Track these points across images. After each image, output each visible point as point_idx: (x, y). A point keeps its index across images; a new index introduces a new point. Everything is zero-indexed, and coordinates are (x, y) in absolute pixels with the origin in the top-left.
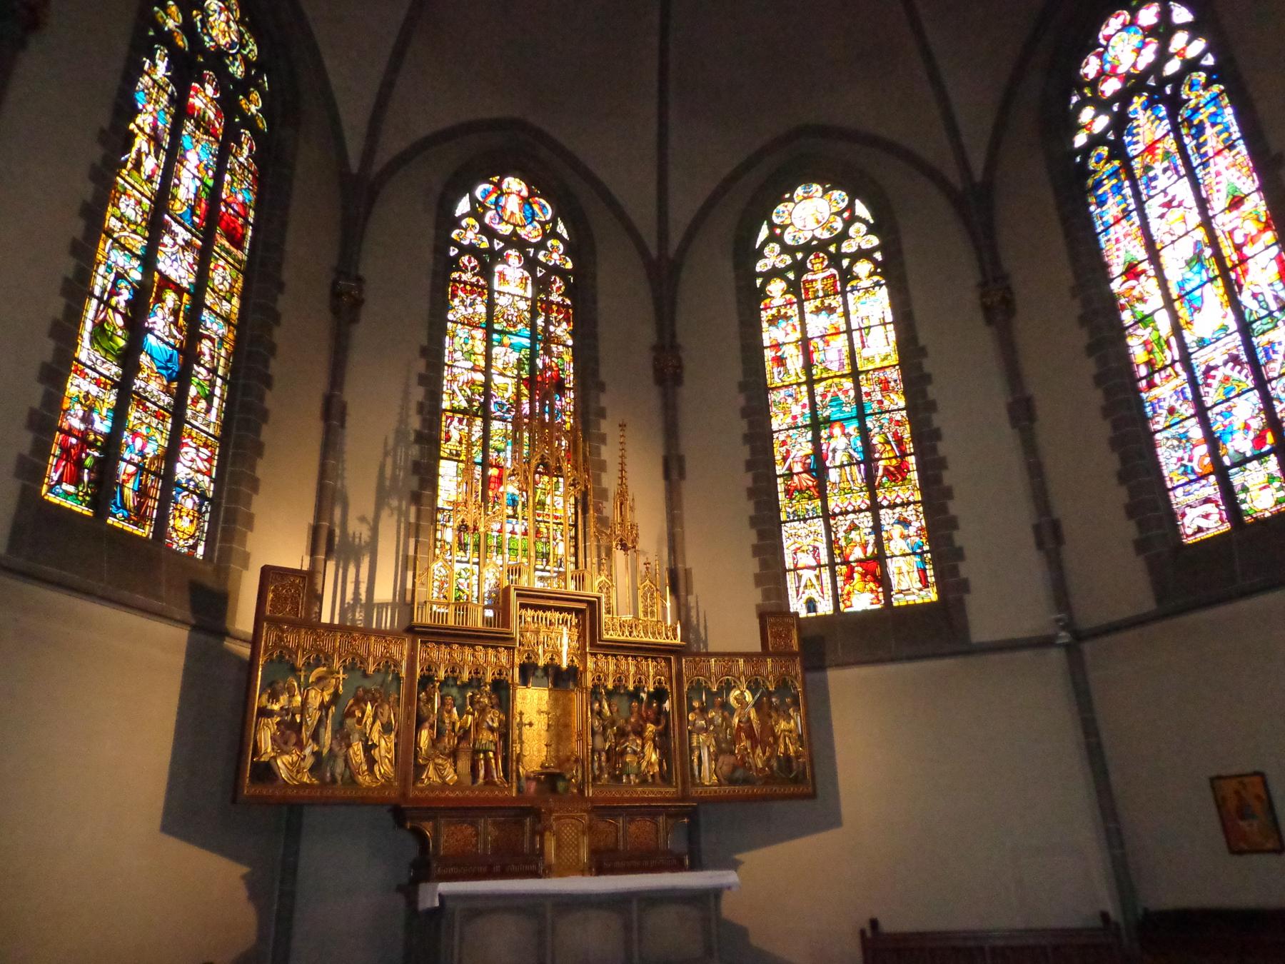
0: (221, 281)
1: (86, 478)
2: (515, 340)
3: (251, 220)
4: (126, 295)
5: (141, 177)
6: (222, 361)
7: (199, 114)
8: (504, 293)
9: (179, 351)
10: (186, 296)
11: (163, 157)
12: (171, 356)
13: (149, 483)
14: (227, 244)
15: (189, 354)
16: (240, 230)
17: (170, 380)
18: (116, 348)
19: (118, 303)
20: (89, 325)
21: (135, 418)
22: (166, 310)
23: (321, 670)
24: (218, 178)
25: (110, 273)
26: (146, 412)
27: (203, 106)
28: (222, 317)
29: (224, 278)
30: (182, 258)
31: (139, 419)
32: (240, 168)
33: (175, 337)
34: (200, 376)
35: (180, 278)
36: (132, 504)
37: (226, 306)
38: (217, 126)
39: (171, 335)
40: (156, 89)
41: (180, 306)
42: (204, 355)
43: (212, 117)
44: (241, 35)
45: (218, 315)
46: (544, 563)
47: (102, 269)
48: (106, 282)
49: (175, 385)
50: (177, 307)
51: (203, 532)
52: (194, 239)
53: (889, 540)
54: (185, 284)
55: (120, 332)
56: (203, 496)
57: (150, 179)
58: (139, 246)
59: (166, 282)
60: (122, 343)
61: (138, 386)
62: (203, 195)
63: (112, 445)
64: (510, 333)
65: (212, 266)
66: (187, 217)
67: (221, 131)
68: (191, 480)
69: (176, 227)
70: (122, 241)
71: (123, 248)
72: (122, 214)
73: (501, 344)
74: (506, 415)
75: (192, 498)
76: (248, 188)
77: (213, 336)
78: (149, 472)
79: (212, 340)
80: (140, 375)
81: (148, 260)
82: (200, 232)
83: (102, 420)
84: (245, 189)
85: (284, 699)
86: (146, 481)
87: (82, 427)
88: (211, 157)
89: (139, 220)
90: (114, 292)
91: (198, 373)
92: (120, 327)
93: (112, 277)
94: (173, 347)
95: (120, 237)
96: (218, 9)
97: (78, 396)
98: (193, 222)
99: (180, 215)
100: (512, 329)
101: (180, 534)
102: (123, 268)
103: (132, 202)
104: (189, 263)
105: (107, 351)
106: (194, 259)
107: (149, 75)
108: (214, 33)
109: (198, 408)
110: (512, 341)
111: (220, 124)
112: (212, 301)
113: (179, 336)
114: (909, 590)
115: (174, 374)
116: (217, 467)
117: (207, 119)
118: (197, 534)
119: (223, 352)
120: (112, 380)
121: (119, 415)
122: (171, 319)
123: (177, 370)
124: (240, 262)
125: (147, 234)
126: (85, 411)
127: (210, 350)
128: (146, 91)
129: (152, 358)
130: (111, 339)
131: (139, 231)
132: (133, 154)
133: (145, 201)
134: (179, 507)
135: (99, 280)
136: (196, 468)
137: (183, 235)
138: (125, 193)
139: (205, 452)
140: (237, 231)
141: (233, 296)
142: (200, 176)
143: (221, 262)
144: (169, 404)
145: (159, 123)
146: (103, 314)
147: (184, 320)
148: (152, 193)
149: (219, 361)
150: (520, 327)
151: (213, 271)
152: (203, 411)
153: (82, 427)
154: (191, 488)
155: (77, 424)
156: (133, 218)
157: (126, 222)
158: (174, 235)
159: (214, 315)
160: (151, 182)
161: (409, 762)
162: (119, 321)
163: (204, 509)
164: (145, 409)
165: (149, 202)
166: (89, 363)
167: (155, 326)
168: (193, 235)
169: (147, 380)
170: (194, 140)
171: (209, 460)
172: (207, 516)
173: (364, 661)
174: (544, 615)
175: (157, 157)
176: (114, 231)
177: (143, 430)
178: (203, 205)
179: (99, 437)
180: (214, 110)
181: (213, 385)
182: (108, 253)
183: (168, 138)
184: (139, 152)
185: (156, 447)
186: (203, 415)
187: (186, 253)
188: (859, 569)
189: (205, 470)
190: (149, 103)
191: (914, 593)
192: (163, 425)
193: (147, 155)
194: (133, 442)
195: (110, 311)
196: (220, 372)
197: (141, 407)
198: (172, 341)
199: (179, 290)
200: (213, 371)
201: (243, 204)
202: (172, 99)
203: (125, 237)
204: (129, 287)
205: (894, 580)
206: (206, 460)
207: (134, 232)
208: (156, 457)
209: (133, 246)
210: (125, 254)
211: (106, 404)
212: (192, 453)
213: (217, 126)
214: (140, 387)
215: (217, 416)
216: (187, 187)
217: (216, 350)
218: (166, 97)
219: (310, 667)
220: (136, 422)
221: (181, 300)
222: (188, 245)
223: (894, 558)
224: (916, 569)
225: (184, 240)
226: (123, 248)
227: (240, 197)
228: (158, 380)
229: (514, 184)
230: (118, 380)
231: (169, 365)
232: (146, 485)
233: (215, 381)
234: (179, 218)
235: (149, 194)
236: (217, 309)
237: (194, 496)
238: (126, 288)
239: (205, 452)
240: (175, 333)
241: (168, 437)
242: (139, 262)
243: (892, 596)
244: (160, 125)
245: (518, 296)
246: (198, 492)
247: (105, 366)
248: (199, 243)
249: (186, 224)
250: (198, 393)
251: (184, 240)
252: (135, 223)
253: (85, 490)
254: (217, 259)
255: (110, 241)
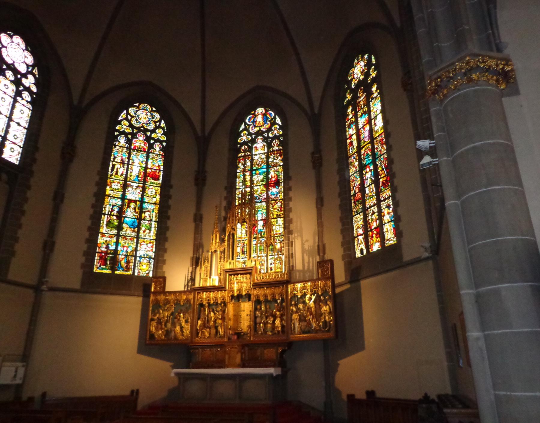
0: (151, 192)
1: (108, 263)
2: (261, 171)
3: (162, 169)
4: (116, 210)
5: (118, 176)
6: (154, 216)
7: (137, 147)
8: (256, 155)
9: (137, 219)
10: (138, 203)
11: (126, 166)
12: (134, 221)
13: (130, 259)
14: (153, 181)
15: (140, 219)
16: (158, 174)
17: (134, 228)
18: (114, 225)
19: (114, 213)
20: (105, 223)
21: (123, 242)
22: (131, 209)
23: (168, 306)
24: (147, 163)
25: (110, 206)
26: (127, 240)
27: (139, 144)
28: (153, 203)
29: (152, 192)
30: (136, 192)
31: (125, 242)
32: (156, 155)
33: (135, 215)
34: (145, 224)
35: (135, 198)
36: (124, 266)
37: (154, 199)
38: (145, 147)
39: (134, 215)
40: (121, 148)
41: (136, 206)
42: (146, 217)
43: (143, 145)
44: (152, 115)
45: (151, 203)
46: (272, 252)
47: (108, 206)
48: (109, 209)
49: (137, 229)
50: (135, 207)
51: (151, 268)
52: (140, 184)
53: (384, 216)
54: (137, 199)
55: (115, 221)
56: (150, 258)
57: (122, 175)
58: (120, 195)
59: (130, 201)
60: (116, 224)
61: (123, 233)
62: (142, 170)
63: (116, 251)
64: (259, 169)
65: (147, 190)
66: (137, 179)
67: (147, 148)
68: (146, 254)
69: (132, 184)
70: (114, 196)
71: (114, 197)
72: (113, 189)
73: (256, 174)
74: (258, 200)
75: (146, 259)
76: (160, 160)
77: (150, 210)
78: (129, 256)
79: (149, 211)
80: (123, 230)
81: (123, 198)
82: (142, 181)
83: (112, 246)
84: (159, 161)
85: (157, 315)
86: (129, 258)
87: (106, 250)
88: (144, 158)
89: (119, 187)
90: (112, 210)
91: (145, 223)
92: (115, 220)
93: (111, 207)
94: (134, 218)
95: (113, 195)
96: (142, 112)
97: (103, 242)
98: (139, 180)
99: (134, 180)
100: (259, 167)
101: (143, 271)
102: (115, 203)
103: (116, 183)
104: (138, 192)
105: (111, 227)
106: (140, 190)
107: (118, 146)
108: (141, 121)
109: (146, 233)
110: (260, 172)
111: (146, 146)
112: (148, 200)
113: (136, 215)
114: (390, 239)
115: (136, 226)
116: (155, 248)
117: (141, 147)
118: (149, 269)
119: (154, 214)
120: (114, 235)
121: (117, 243)
122: (134, 211)
123: (136, 225)
124: (159, 184)
125: (122, 190)
126: (106, 246)
127: (149, 215)
128: (118, 151)
129: (127, 224)
130: (113, 224)
131: (119, 191)
132: (115, 170)
133: (120, 181)
134: (141, 263)
135: (107, 209)
136: (147, 250)
137: (135, 185)
138: (114, 182)
139: (150, 245)
140: (157, 175)
141: (156, 195)
142: (140, 165)
143: (151, 187)
144: (135, 235)
145: (123, 157)
146: (110, 218)
147: (138, 209)
148: (123, 178)
149: (152, 216)
150: (262, 165)
151: (148, 191)
152: (148, 233)
153: (106, 250)
154: (145, 256)
155: (104, 249)
156: (117, 188)
157: (115, 190)
158: (132, 187)
159: (149, 204)
160: (122, 175)
161: (195, 332)
162: (115, 218)
163: (151, 261)
164: (126, 239)
165: (122, 181)
166: (106, 232)
167: (128, 215)
168: (139, 183)
169: (126, 231)
170: (137, 156)
171: (152, 247)
172: (152, 263)
173: (180, 301)
174: (243, 276)
175: (124, 167)
176: (111, 194)
177: (126, 245)
178: (142, 173)
179: (111, 251)
180: (143, 143)
181: (151, 224)
182: (109, 201)
183: (127, 160)
184: (117, 169)
185: (132, 248)
186: (148, 234)
187: (137, 190)
188: (375, 232)
189: (150, 250)
190: (119, 154)
191: (392, 240)
192: (133, 242)
193: (120, 168)
194: (123, 249)
195: (112, 216)
196: (154, 220)
197: (125, 239)
198: (134, 217)
199: (135, 201)
200: (151, 220)
201: (159, 166)
202: (127, 148)
203: (115, 194)
204: (117, 207)
205: (386, 235)
206: (151, 247)
207: (118, 192)
208: (132, 251)
209: (118, 196)
210: (115, 199)
211: (113, 242)
212: (145, 246)
213: (145, 147)
214: (124, 234)
215: (154, 233)
216: (135, 170)
217: (151, 214)
218: (125, 149)
219: (165, 305)
220: (124, 243)
221: (136, 204)
222: (137, 187)
223: (386, 225)
224: (392, 229)
225: (136, 186)
226: (114, 197)
227: (157, 165)
228: (130, 230)
229: (261, 110)
230: (116, 234)
231: (134, 224)
232: (129, 260)
233: (152, 223)
234: (133, 181)
235: (122, 179)
236: (151, 202)
237: (147, 259)
238: (116, 208)
239: (151, 245)
240: (135, 214)
241: (135, 244)
242: (120, 199)
243: (385, 243)
244: (124, 158)
245: (262, 153)
246: (148, 257)
247: (111, 231)
248: (142, 185)
249: (137, 182)
250: (145, 228)
251: (136, 186)
252: (118, 189)
253: (108, 266)
254: (149, 187)
255: (110, 197)
